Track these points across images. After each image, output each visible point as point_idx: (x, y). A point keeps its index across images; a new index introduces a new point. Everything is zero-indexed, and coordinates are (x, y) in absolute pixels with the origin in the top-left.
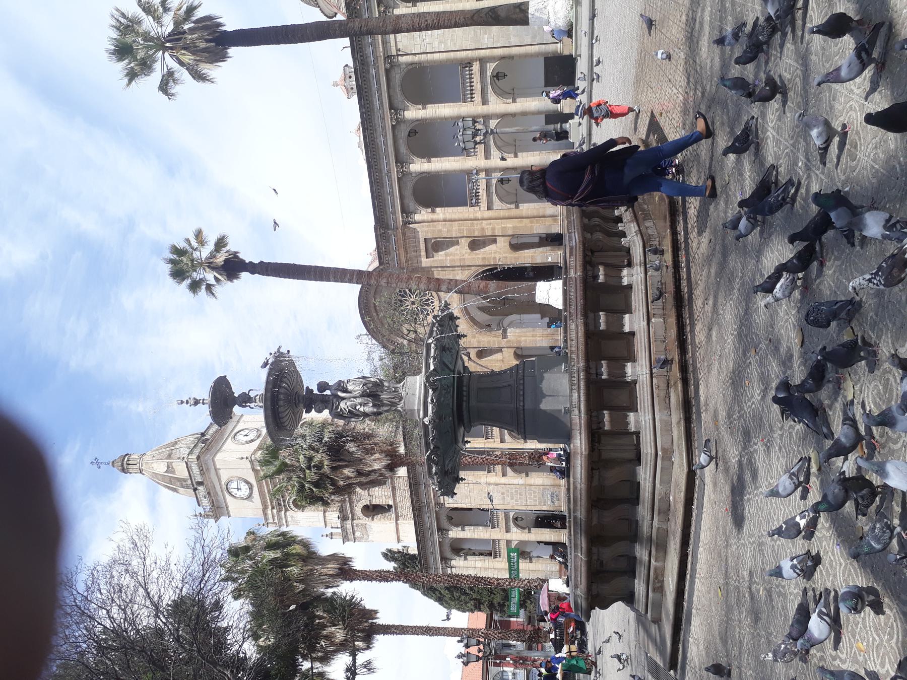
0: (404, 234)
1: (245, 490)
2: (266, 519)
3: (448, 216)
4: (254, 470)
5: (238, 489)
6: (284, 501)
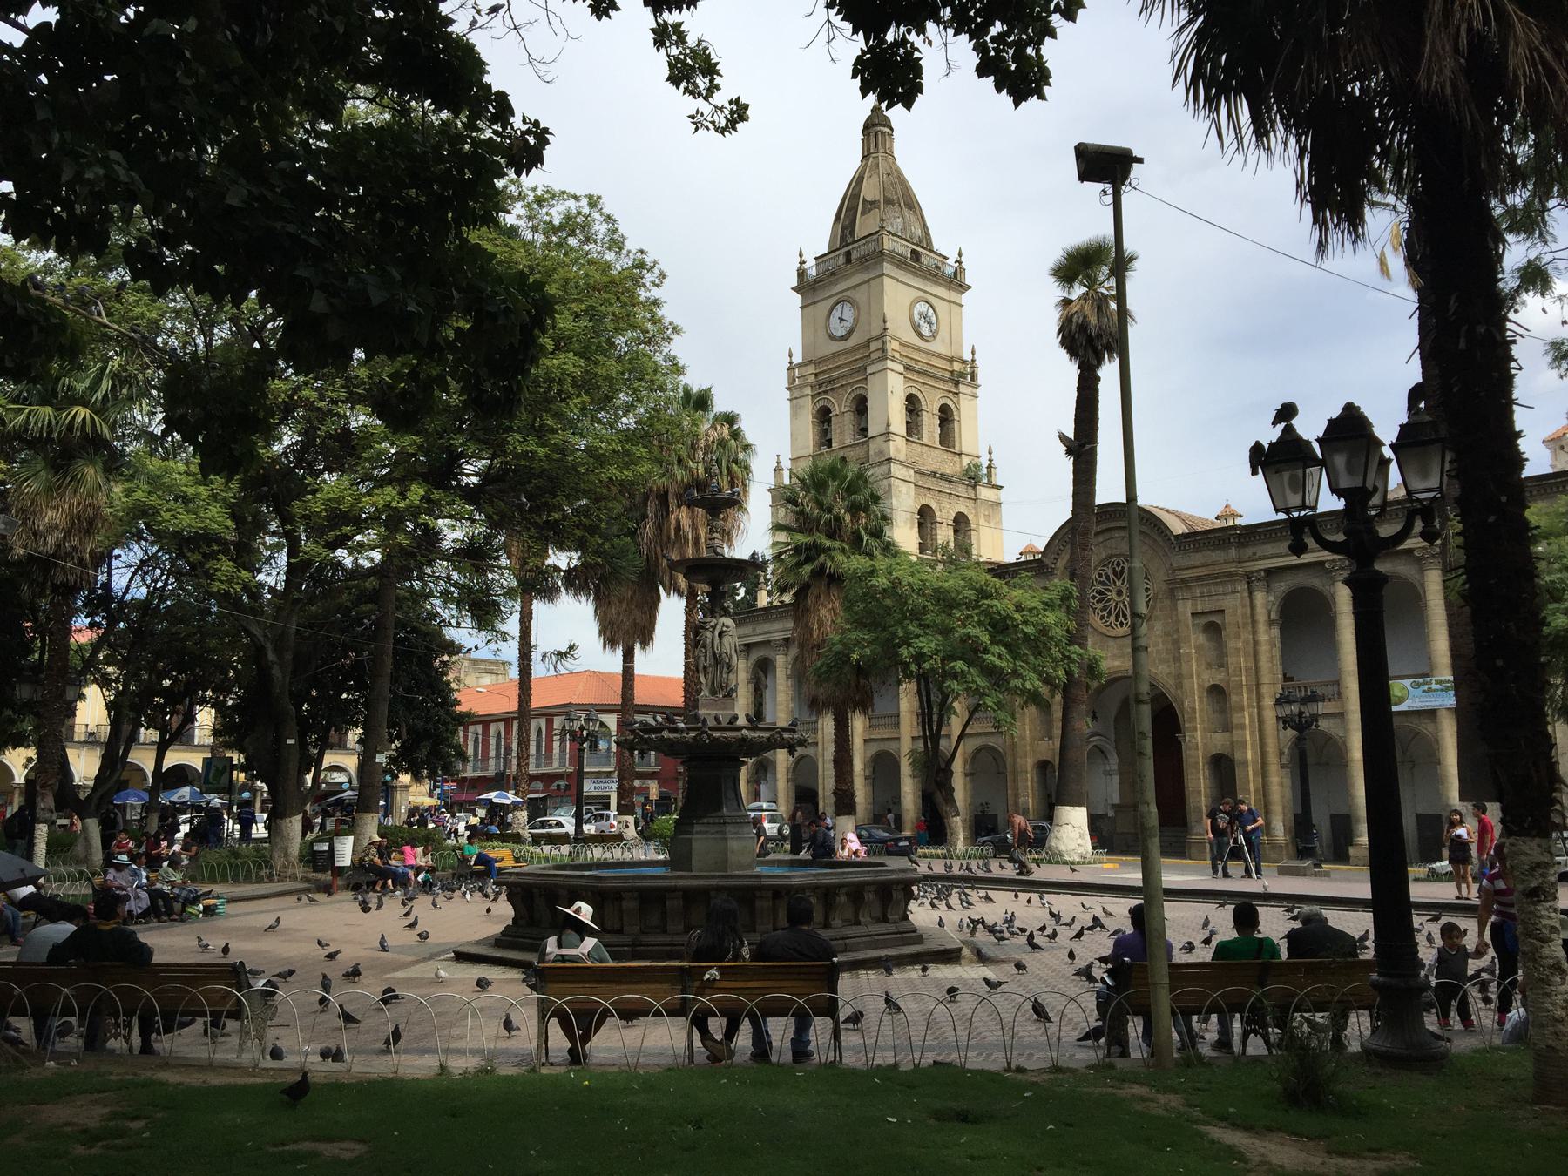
0: (1230, 574)
1: (840, 331)
2: (799, 366)
3: (1264, 649)
4: (870, 341)
5: (841, 319)
6: (826, 392)
